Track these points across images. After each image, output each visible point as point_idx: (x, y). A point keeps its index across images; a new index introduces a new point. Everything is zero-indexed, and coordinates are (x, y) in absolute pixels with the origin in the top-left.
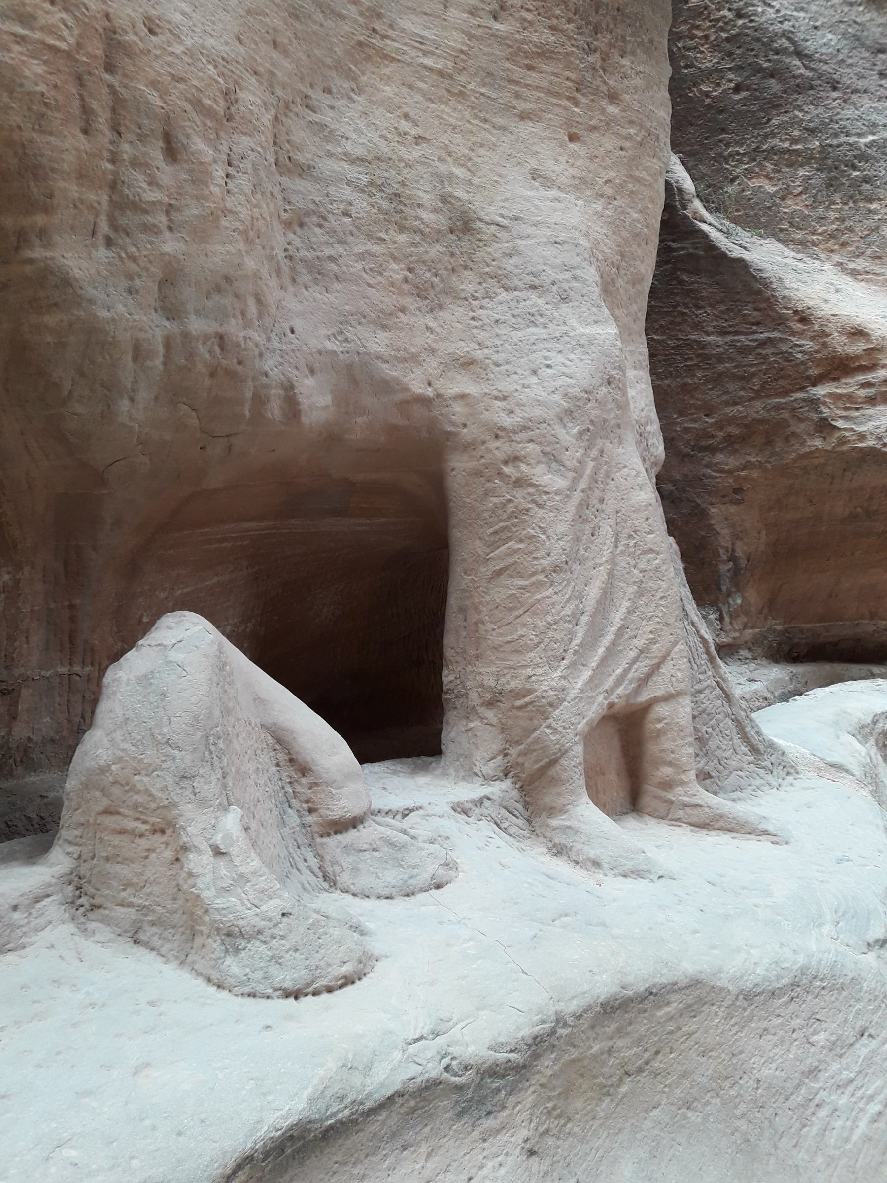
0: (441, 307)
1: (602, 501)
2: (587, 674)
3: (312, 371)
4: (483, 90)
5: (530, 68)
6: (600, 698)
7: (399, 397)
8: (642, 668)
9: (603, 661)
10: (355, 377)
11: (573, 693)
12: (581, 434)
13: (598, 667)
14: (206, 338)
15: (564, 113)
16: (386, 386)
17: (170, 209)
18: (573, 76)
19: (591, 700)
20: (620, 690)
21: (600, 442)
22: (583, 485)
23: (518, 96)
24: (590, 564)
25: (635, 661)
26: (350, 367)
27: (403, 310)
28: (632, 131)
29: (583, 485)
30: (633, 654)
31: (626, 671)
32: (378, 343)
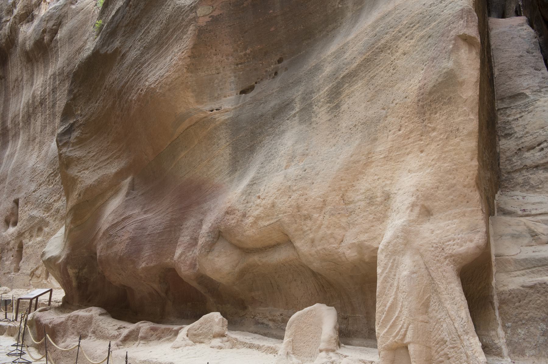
0: (383, 222)
1: (395, 275)
2: (386, 330)
3: (350, 248)
4: (398, 153)
5: (409, 138)
6: (391, 339)
7: (371, 249)
8: (403, 330)
9: (391, 327)
10: (360, 247)
11: (381, 335)
12: (386, 256)
13: (389, 328)
14: (321, 250)
15: (417, 146)
16: (368, 248)
17: (310, 229)
18: (419, 133)
19: (388, 339)
20: (397, 338)
21: (393, 257)
22: (387, 271)
23: (406, 149)
24: (389, 296)
25: (401, 329)
26: (359, 245)
27: (373, 226)
28: (442, 137)
29: (387, 271)
30: (400, 326)
31: (399, 331)
32: (363, 237)
